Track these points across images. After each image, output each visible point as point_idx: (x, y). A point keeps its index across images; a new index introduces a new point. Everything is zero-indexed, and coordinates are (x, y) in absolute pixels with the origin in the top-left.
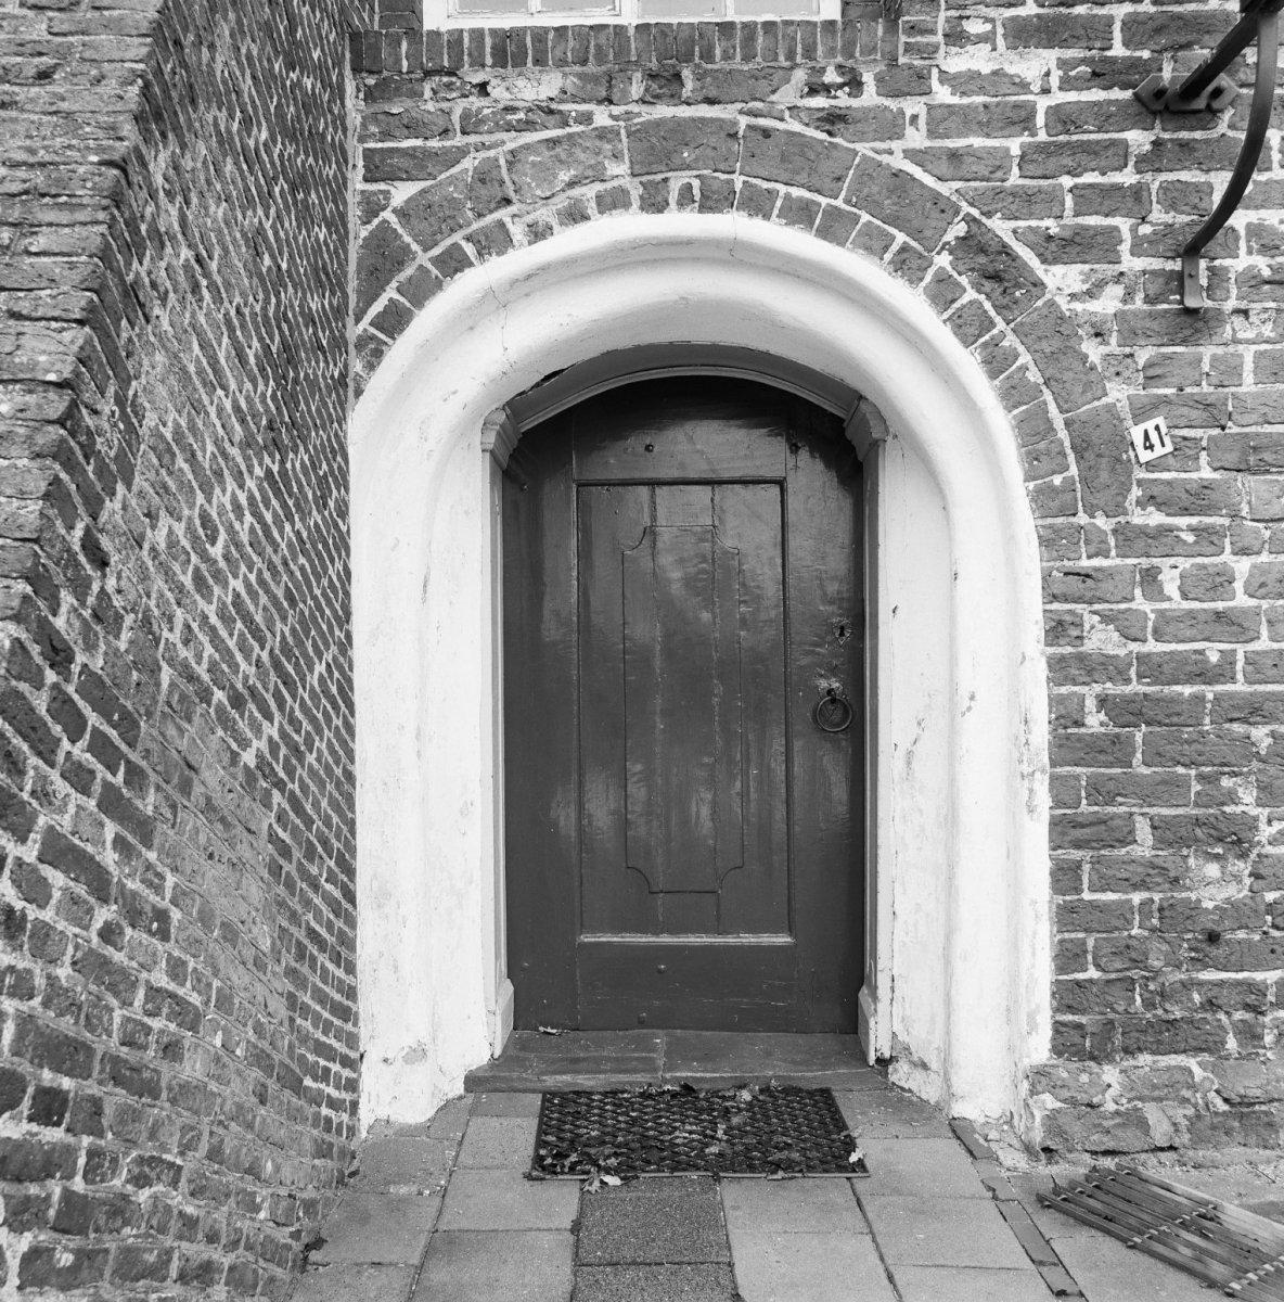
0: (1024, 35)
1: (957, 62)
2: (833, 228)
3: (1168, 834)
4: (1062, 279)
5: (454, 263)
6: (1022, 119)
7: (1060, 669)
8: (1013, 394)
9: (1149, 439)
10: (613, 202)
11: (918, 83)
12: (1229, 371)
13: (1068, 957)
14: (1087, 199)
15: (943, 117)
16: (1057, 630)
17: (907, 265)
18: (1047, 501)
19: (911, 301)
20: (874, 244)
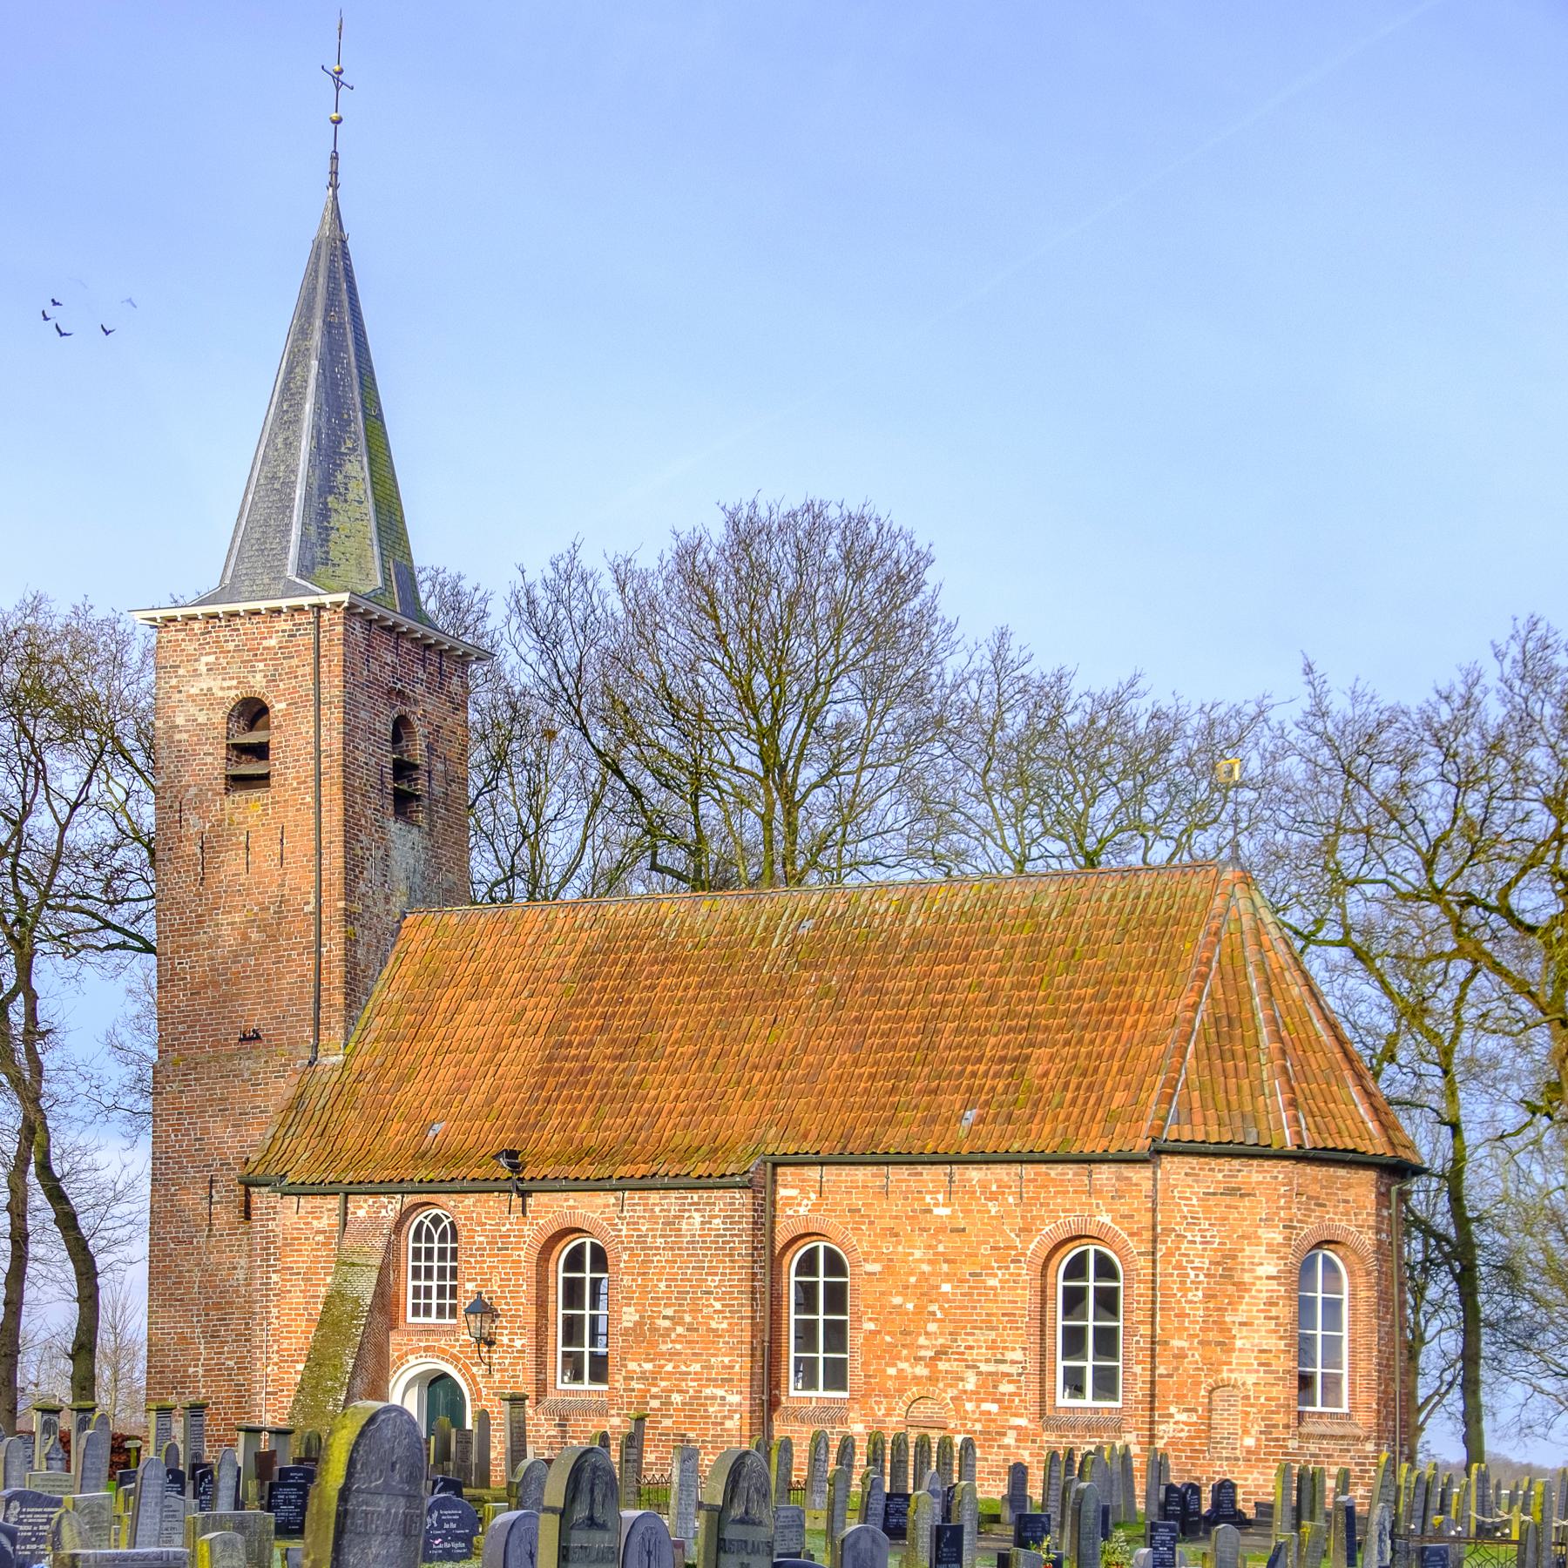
1: (462, 1337)
4: (475, 1369)
9: (484, 1391)
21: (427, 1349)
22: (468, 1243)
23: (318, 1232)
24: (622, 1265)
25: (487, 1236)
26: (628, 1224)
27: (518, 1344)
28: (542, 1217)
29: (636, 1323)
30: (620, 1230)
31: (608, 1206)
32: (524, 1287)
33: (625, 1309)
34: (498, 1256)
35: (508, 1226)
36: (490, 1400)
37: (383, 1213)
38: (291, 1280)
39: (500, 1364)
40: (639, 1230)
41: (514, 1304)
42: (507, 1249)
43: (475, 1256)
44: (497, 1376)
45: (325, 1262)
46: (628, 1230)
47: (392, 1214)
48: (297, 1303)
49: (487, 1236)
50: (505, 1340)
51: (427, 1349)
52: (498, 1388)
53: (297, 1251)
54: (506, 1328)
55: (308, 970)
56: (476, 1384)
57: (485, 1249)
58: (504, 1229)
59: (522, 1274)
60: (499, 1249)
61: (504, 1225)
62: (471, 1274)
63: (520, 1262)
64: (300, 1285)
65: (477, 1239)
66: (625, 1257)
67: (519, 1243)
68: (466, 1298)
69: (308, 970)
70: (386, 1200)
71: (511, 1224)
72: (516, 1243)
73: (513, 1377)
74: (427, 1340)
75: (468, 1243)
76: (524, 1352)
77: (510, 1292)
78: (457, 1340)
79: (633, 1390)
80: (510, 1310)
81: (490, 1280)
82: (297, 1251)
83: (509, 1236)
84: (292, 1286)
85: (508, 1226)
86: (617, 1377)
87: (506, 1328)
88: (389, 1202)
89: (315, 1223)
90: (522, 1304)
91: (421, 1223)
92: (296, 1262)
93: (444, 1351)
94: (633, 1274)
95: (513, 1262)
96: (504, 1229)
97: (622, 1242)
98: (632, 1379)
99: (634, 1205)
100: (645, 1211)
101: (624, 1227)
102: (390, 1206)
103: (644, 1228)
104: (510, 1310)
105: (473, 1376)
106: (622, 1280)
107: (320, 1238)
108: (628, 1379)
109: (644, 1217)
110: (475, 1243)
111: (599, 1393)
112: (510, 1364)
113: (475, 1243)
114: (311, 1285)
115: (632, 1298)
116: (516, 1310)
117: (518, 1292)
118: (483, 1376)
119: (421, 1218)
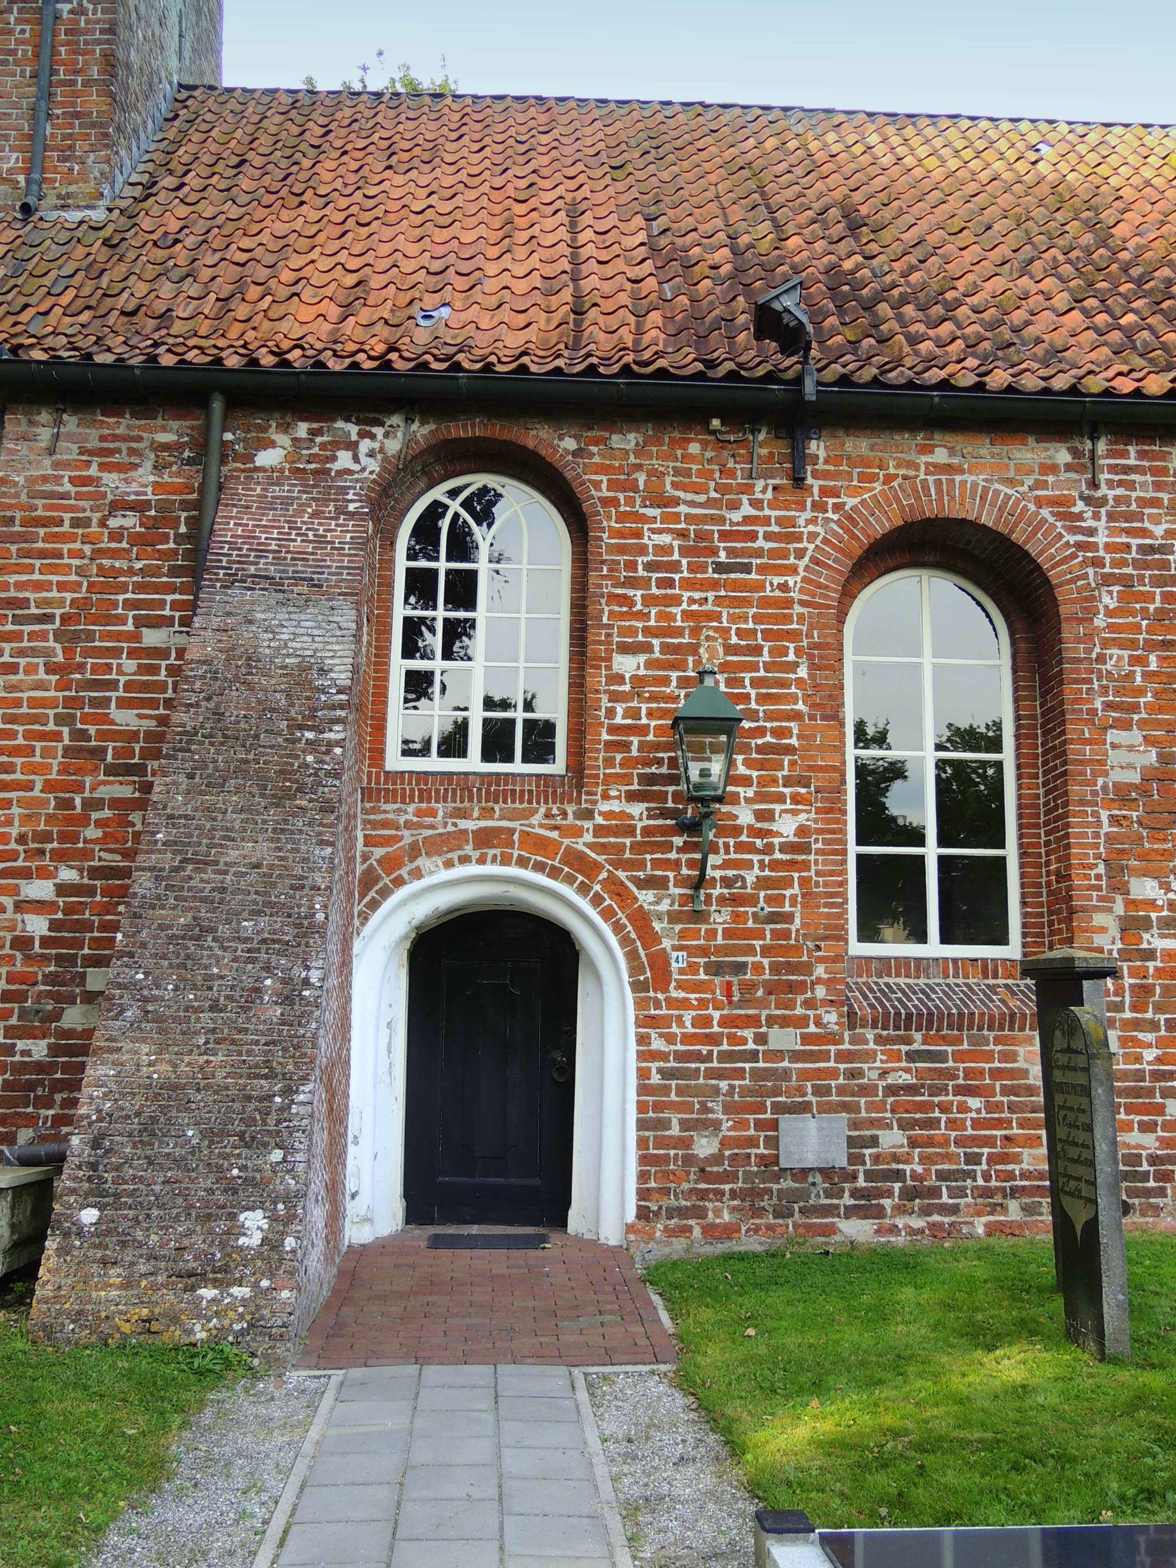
0: (632, 797)
1: (605, 807)
2: (554, 873)
3: (685, 1125)
4: (645, 897)
5: (399, 882)
6: (631, 831)
7: (642, 1056)
8: (625, 941)
9: (678, 961)
10: (465, 860)
11: (588, 815)
12: (712, 934)
13: (643, 1176)
14: (656, 863)
15: (599, 830)
16: (642, 1039)
17: (583, 889)
18: (637, 986)
19: (584, 904)
20: (570, 880)
21: (484, 839)
22: (622, 550)
23: (119, 506)
24: (1100, 621)
25: (683, 534)
26: (1111, 517)
27: (786, 827)
28: (854, 492)
29: (1148, 776)
30: (1092, 532)
31: (1053, 469)
32: (803, 672)
33: (1112, 736)
34: (714, 585)
35: (747, 510)
36: (698, 987)
37: (344, 459)
38: (16, 636)
39: (727, 882)
40: (1144, 533)
41: (769, 717)
42: (746, 568)
43: (645, 583)
44: (721, 918)
45: (139, 588)
46: (1112, 532)
47: (373, 465)
48: (33, 703)
49: (683, 534)
50: (745, 816)
51: (484, 839)
52: (719, 950)
53: (43, 554)
54: (746, 781)
55: (19, 42)
56: (649, 936)
57: (675, 567)
58: (736, 516)
59: (793, 636)
60: (720, 568)
61: (735, 506)
62: (632, 631)
63: (789, 603)
64: (48, 653)
65: (651, 540)
66: (1109, 601)
67: (784, 554)
68: (615, 697)
69: (19, 42)
70: (353, 430)
71: (756, 504)
72: (773, 554)
73: (773, 918)
74: (487, 813)
75: (622, 550)
76: (804, 848)
77: (755, 683)
78: (588, 815)
79: (1150, 955)
80: (761, 732)
81: (694, 649)
82: (43, 554)
83: (753, 536)
84: (22, 653)
85: (747, 510)
86: (1099, 919)
87: (746, 781)
88: (362, 435)
89: (111, 480)
90: (796, 716)
91: (436, 510)
92: (39, 586)
93: (541, 844)
94: (1133, 644)
95: (765, 602)
96: (736, 516)
97: (1098, 563)
98: (1146, 924)
99: (1127, 470)
100: (1158, 486)
101: (1102, 524)
102: (365, 445)
103: (1159, 530)
104: (761, 732)
105: (642, 919)
106: (1101, 659)
107: (130, 521)
108: (1132, 926)
109: (1155, 503)
110: (643, 550)
111: (986, 968)
112: (762, 883)
113: (643, 550)
114: (87, 653)
115: (1135, 708)
116: (779, 733)
117: (783, 684)
118: (673, 917)
119: (438, 493)
